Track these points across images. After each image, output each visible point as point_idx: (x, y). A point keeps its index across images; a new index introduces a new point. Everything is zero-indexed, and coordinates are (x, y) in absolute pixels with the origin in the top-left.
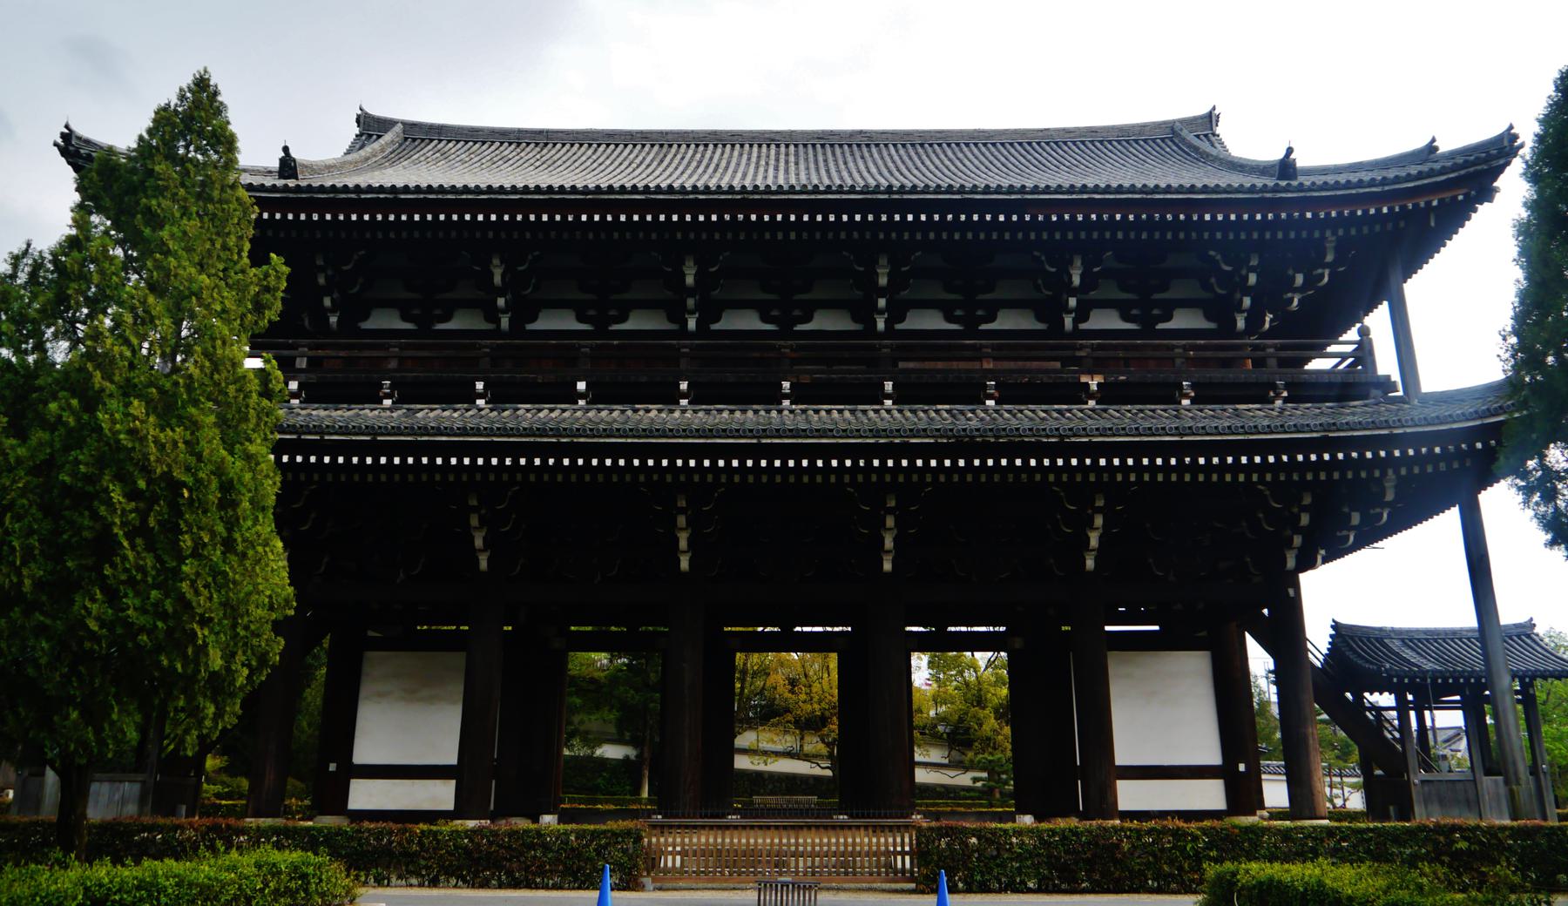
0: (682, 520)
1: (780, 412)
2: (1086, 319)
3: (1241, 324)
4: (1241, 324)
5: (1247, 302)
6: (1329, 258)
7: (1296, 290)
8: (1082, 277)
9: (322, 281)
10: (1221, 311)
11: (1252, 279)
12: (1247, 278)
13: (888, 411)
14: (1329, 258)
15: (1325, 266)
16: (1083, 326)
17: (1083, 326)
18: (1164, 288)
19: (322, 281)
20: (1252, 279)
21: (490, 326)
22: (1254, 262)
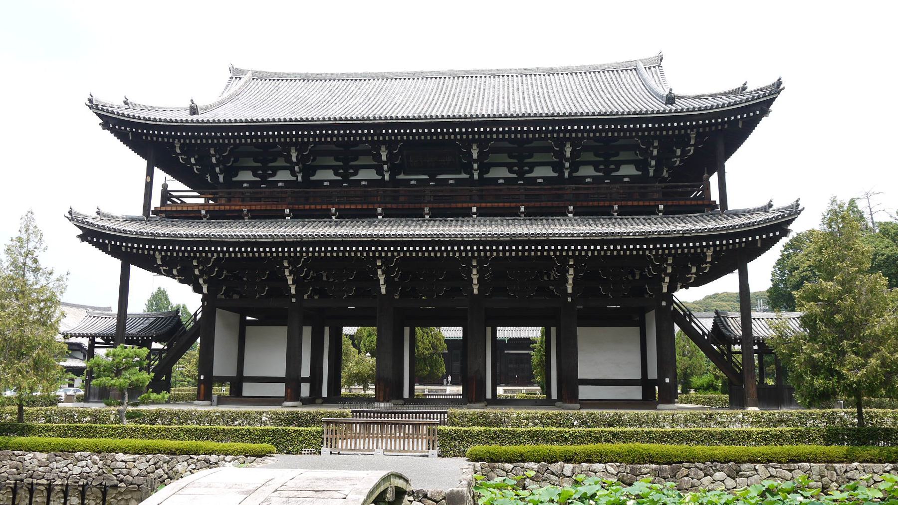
0: (380, 272)
1: (424, 221)
2: (577, 171)
3: (651, 174)
4: (651, 174)
5: (653, 163)
6: (692, 142)
7: (677, 157)
8: (572, 152)
9: (214, 160)
10: (642, 165)
11: (655, 152)
12: (652, 152)
13: (474, 221)
14: (692, 142)
15: (691, 146)
16: (574, 174)
17: (574, 174)
18: (617, 155)
19: (214, 160)
20: (655, 152)
21: (294, 178)
22: (656, 144)
